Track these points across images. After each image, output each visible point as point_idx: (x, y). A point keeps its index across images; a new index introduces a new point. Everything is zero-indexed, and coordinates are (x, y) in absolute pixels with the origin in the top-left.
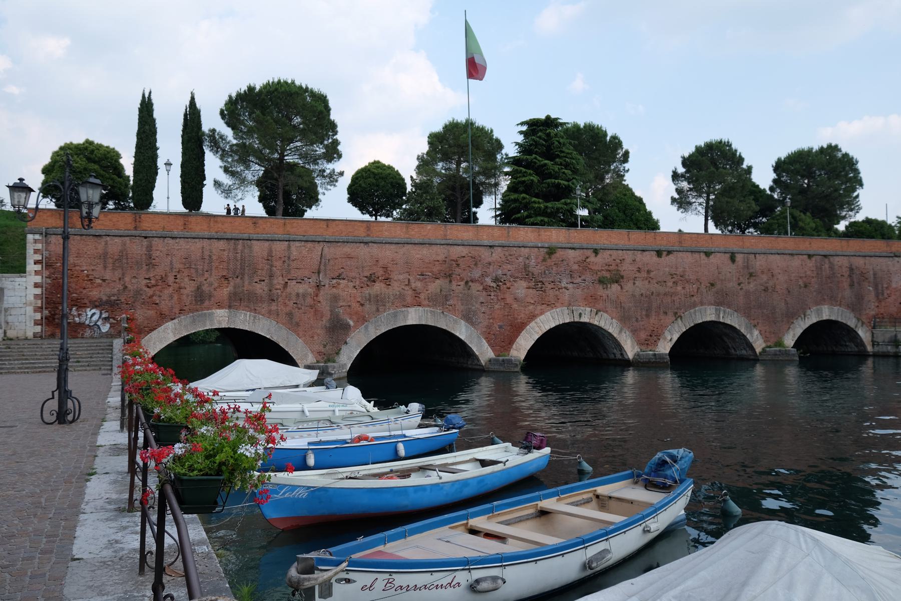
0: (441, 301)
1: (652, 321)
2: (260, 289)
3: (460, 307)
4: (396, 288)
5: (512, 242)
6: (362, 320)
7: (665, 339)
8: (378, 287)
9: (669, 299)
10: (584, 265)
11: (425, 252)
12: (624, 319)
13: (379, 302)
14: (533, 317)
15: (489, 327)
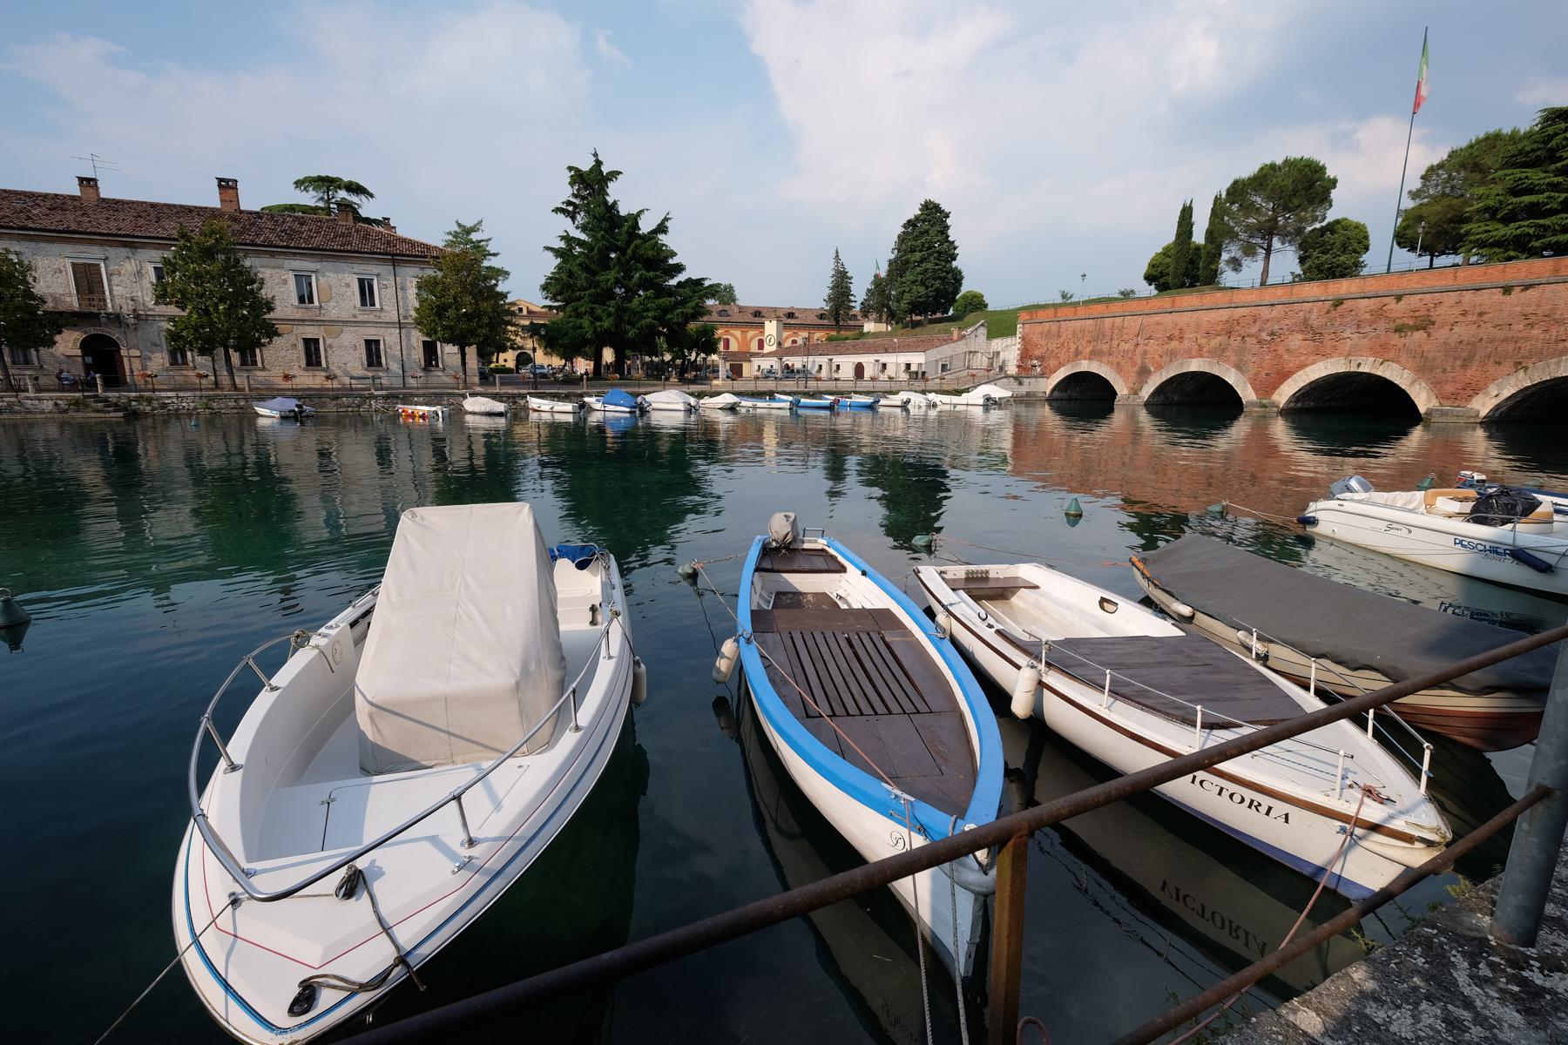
0: (1219, 353)
1: (1470, 372)
2: (1105, 347)
3: (1234, 358)
4: (1186, 344)
5: (1294, 299)
6: (1160, 367)
7: (1487, 394)
8: (1174, 344)
9: (1511, 347)
10: (1379, 314)
11: (1213, 315)
12: (1424, 368)
13: (1173, 355)
14: (1302, 366)
15: (1257, 374)
